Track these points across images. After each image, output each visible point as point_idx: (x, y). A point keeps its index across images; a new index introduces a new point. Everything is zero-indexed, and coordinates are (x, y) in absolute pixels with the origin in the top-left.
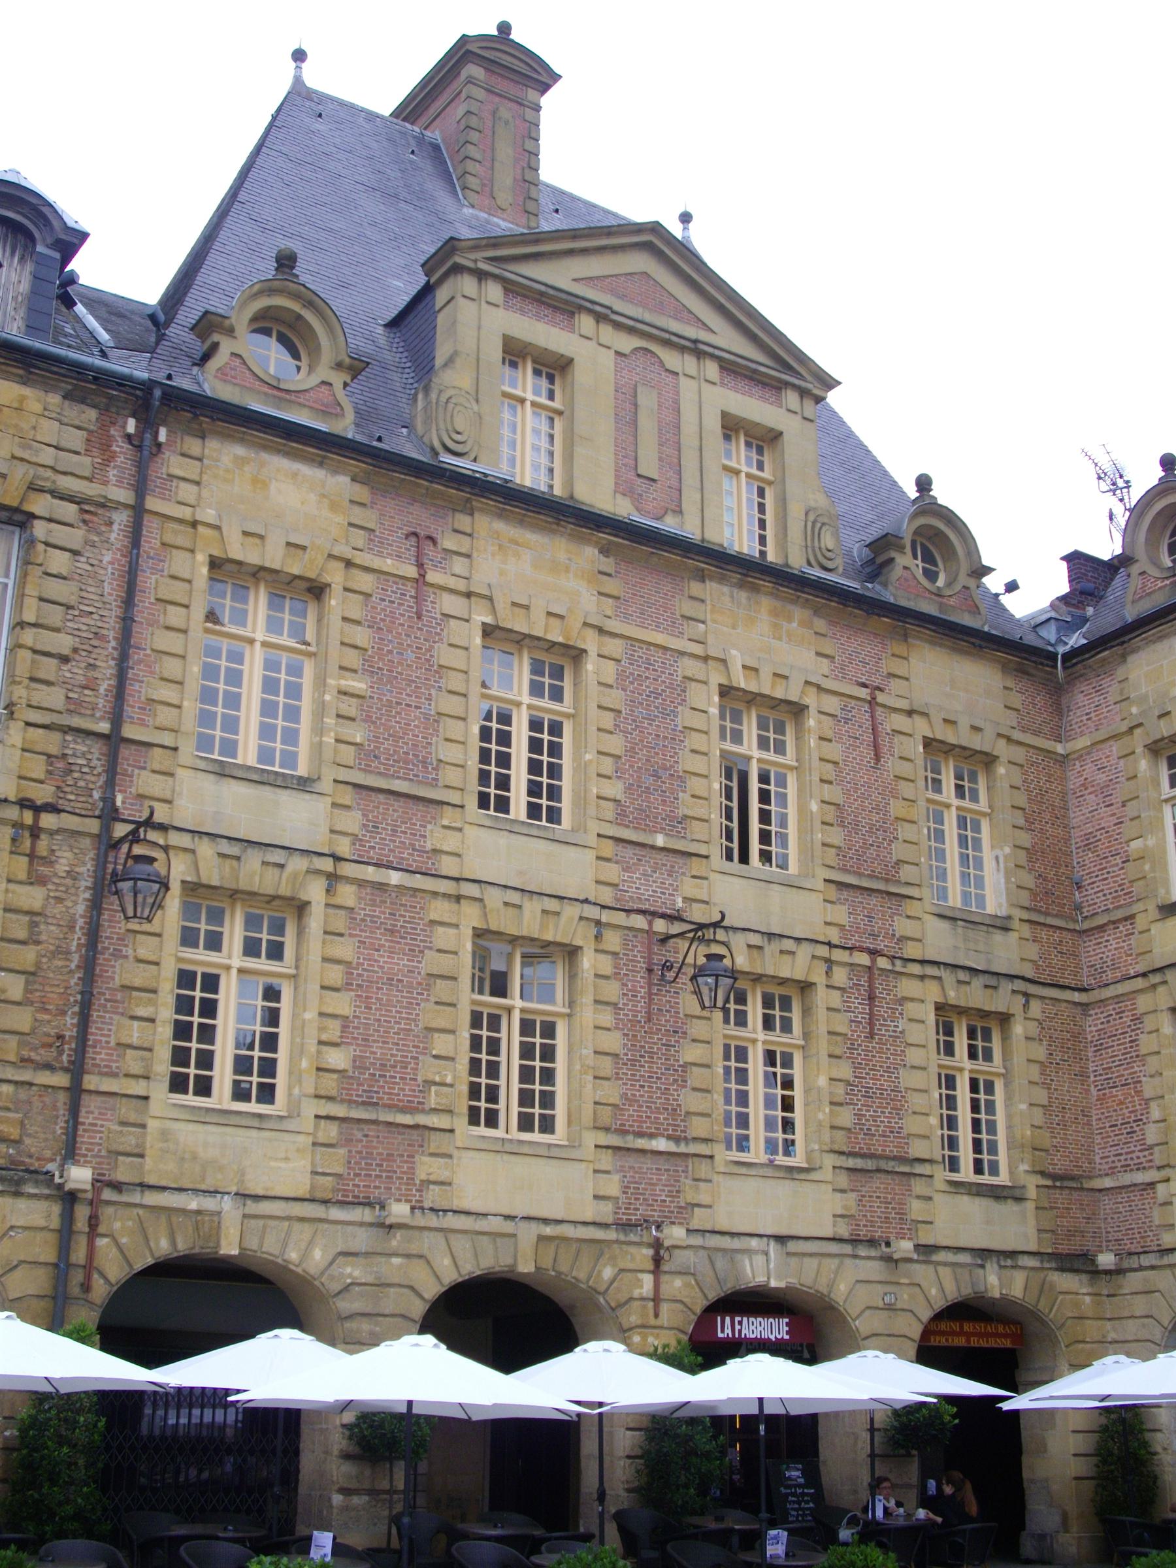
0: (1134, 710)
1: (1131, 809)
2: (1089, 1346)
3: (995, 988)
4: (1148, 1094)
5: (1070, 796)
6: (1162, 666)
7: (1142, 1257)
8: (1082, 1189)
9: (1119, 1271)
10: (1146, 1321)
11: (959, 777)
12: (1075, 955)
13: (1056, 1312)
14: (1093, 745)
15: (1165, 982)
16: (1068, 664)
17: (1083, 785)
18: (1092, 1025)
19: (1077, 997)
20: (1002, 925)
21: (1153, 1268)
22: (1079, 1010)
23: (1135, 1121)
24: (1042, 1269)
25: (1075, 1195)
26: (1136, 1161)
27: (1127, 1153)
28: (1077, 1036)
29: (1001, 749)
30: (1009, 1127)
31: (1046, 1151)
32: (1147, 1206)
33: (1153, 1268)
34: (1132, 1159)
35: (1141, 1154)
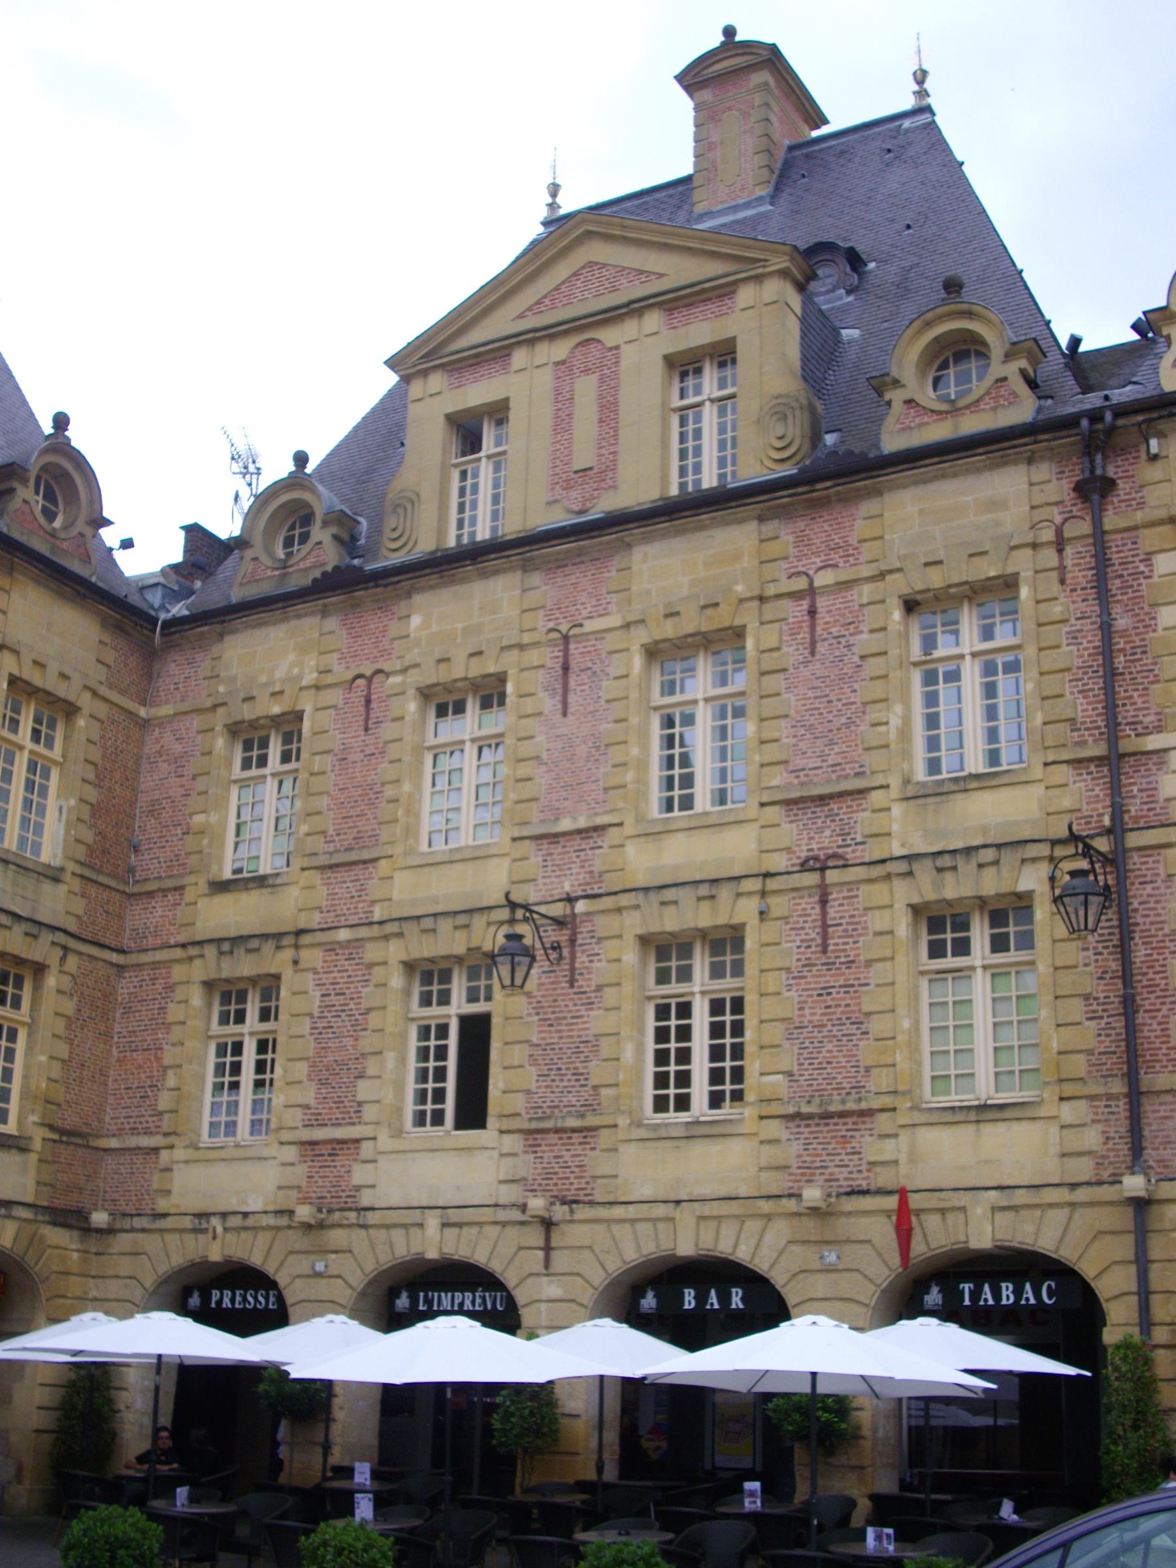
0: (221, 689)
2: (69, 1302)
3: (35, 937)
4: (167, 1060)
5: (144, 761)
6: (255, 652)
7: (135, 1219)
8: (87, 1147)
9: (110, 1231)
10: (129, 1281)
11: (38, 720)
12: (120, 917)
14: (176, 714)
15: (202, 956)
16: (167, 632)
17: (159, 752)
18: (125, 987)
19: (115, 957)
20: (54, 876)
21: (144, 1230)
22: (113, 971)
23: (150, 1086)
24: (35, 1221)
25: (80, 1152)
26: (145, 1125)
27: (137, 1117)
28: (108, 996)
29: (85, 701)
30: (26, 1077)
31: (59, 1105)
32: (147, 1171)
33: (144, 1230)
34: (141, 1123)
35: (150, 1119)
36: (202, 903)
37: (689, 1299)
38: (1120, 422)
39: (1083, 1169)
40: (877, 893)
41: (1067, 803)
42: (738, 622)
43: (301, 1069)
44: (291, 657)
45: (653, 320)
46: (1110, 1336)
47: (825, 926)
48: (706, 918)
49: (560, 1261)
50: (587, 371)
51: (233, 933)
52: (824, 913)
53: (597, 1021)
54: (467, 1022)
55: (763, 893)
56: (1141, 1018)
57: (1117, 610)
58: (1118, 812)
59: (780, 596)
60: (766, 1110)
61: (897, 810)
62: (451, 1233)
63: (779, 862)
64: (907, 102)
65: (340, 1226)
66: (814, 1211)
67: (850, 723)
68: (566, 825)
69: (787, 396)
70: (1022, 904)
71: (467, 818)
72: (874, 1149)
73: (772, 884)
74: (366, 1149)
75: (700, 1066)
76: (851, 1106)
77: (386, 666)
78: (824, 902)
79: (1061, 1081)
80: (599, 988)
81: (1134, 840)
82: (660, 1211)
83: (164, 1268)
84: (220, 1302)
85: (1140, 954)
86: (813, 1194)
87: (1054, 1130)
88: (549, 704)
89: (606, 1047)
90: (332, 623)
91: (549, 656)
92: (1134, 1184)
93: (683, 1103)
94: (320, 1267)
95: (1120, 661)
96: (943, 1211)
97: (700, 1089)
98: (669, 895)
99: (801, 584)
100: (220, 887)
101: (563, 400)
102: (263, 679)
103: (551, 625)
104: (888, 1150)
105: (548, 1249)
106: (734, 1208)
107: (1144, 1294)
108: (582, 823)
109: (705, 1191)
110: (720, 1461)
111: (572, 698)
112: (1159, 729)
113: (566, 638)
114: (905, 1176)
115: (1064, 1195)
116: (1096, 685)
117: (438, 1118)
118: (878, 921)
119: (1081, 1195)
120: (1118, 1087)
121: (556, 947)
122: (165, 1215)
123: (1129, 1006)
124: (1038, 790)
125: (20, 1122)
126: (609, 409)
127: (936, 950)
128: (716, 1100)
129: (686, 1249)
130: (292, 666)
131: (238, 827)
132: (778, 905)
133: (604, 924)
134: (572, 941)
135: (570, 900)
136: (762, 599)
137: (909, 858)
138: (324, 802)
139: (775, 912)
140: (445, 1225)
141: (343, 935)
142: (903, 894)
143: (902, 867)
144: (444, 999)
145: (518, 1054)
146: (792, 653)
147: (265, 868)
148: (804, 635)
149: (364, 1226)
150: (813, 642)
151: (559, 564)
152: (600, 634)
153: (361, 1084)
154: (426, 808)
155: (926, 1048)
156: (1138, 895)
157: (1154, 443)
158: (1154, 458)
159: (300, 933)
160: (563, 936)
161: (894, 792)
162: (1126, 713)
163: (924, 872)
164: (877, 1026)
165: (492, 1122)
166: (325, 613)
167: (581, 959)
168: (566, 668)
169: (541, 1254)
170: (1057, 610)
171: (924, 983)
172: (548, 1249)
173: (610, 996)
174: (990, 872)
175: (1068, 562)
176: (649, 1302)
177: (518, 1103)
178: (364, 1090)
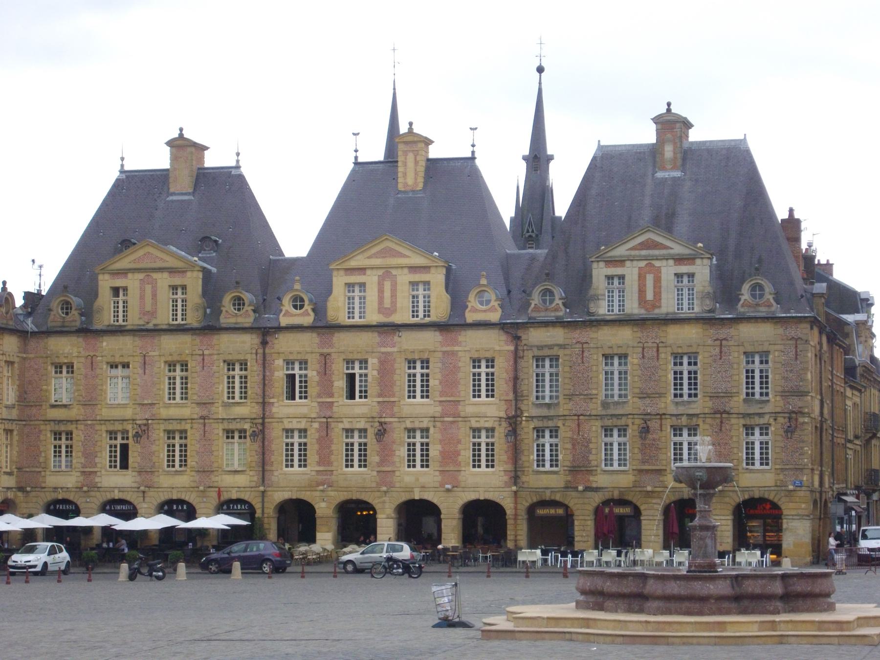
0: (49, 352)
1: (44, 378)
4: (41, 450)
9: (30, 492)
13: (17, 501)
19: (24, 423)
20: (13, 406)
21: (39, 491)
36: (48, 410)
37: (175, 507)
38: (270, 330)
39: (254, 484)
40: (216, 425)
41: (254, 411)
42: (186, 359)
43: (80, 454)
44: (69, 347)
45: (166, 275)
46: (257, 515)
47: (205, 432)
48: (179, 427)
49: (147, 499)
50: (148, 284)
51: (58, 419)
52: (205, 429)
53: (154, 448)
54: (122, 445)
55: (192, 423)
56: (266, 456)
57: (267, 371)
58: (264, 414)
59: (196, 355)
60: (192, 469)
61: (220, 408)
62: (121, 493)
63: (195, 416)
64: (234, 164)
65: (93, 491)
66: (202, 491)
67: (211, 387)
68: (146, 402)
69: (199, 304)
70: (245, 431)
71: (120, 395)
72: (214, 479)
73: (193, 421)
74: (98, 474)
75: (177, 458)
76: (209, 470)
77: (97, 354)
78: (204, 426)
79: (250, 467)
80: (154, 441)
81: (266, 420)
82: (169, 490)
83: (45, 500)
84: (59, 507)
85: (266, 443)
86: (201, 488)
87: (248, 476)
88: (141, 371)
89: (156, 454)
90: (81, 340)
91: (140, 359)
92: (262, 488)
93: (173, 466)
94: (88, 500)
95: (267, 382)
96: (227, 491)
97: (177, 463)
98: (171, 421)
99: (201, 352)
100: (53, 406)
101: (142, 290)
102: (61, 352)
103: (141, 352)
104: (217, 479)
105: (144, 497)
106: (185, 489)
107: (263, 508)
108: (150, 402)
109: (179, 486)
110: (177, 539)
111: (147, 371)
112: (273, 398)
113: (145, 356)
114: (220, 484)
115: (249, 489)
116: (261, 386)
117: (115, 467)
118: (216, 431)
119: (253, 489)
120: (261, 469)
121: (144, 431)
122: (45, 488)
123: (264, 454)
124: (249, 408)
125: (10, 468)
126: (154, 295)
127: (228, 437)
128: (181, 466)
129: (175, 497)
130: (69, 350)
131: (55, 389)
132: (195, 426)
133: (155, 426)
134: (148, 429)
135: (147, 420)
136: (192, 355)
137: (223, 419)
138: (81, 388)
139: (194, 427)
140: (119, 491)
141: (89, 422)
142: (221, 427)
143: (221, 421)
144: (116, 439)
145: (136, 454)
146: (198, 368)
147: (64, 402)
148: (201, 365)
149: (99, 491)
150: (203, 367)
151: (143, 336)
152: (153, 356)
153: (96, 459)
154: (109, 391)
155: (225, 458)
156: (267, 431)
157: (276, 336)
158: (276, 338)
159: (77, 421)
160: (145, 428)
161: (220, 404)
162: (267, 393)
163: (225, 422)
164: (215, 453)
165: (130, 469)
166: (78, 337)
167: (150, 434)
168: (145, 363)
169: (142, 498)
170: (255, 369)
171: (225, 444)
172: (144, 497)
173: (157, 443)
174: (238, 424)
175: (258, 358)
176: (166, 508)
177: (136, 465)
178: (97, 460)
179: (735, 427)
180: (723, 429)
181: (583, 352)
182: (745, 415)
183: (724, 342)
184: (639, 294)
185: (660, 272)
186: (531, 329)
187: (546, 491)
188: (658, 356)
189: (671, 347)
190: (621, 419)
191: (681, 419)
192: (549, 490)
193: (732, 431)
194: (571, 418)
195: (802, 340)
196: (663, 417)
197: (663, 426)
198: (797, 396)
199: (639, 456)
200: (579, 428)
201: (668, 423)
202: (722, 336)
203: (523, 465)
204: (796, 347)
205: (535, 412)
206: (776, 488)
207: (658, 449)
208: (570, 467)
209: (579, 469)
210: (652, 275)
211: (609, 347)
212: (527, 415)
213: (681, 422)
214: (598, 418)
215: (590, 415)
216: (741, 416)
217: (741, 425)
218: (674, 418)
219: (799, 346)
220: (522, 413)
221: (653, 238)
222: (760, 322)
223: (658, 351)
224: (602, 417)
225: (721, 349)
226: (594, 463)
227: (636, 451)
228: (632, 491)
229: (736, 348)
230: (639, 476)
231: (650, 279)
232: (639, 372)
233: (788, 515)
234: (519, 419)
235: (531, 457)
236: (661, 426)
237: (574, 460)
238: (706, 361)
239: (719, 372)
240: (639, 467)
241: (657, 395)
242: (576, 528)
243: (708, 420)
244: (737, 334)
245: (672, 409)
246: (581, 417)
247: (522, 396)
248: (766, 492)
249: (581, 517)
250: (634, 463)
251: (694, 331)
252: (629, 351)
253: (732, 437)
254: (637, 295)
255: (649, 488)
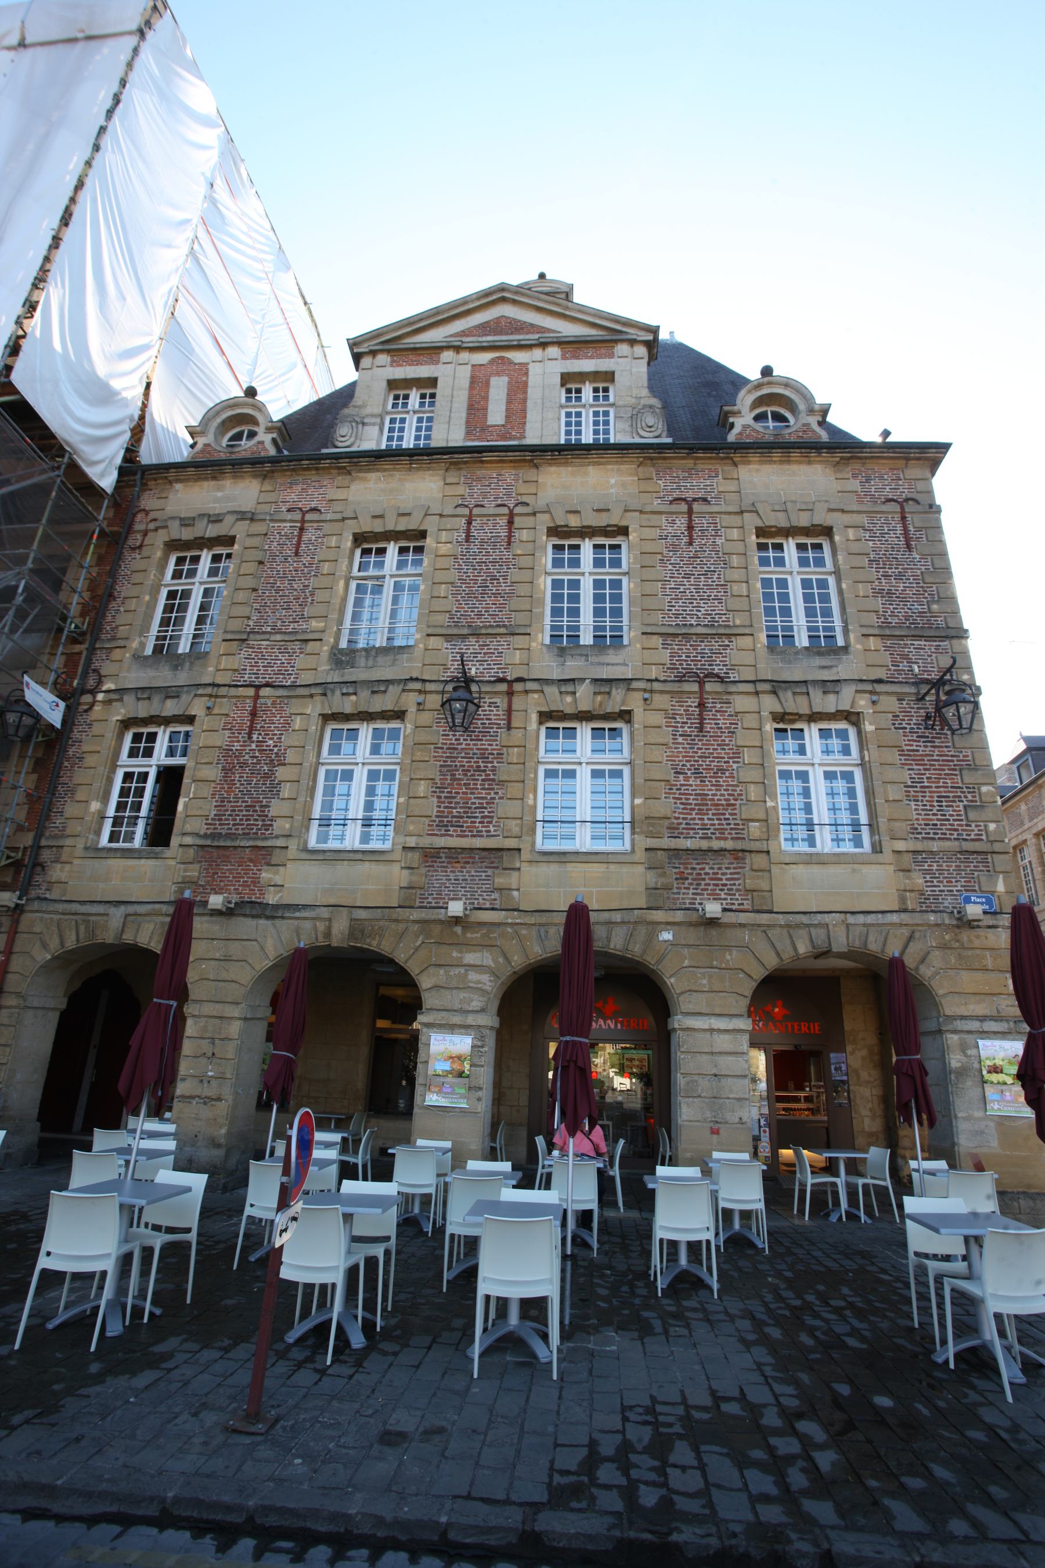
179: (750, 721)
180: (708, 727)
181: (302, 529)
182: (777, 687)
183: (696, 507)
184: (469, 414)
185: (526, 374)
186: (178, 486)
187: (112, 910)
188: (510, 537)
189: (549, 512)
190: (385, 692)
191: (574, 693)
192: (122, 909)
193: (740, 732)
194: (233, 692)
195: (918, 503)
196: (518, 687)
197: (514, 714)
198: (928, 638)
199: (432, 807)
200: (252, 722)
201: (530, 705)
202: (689, 495)
203: (64, 828)
204: (903, 518)
205: (135, 677)
206: (905, 917)
207: (493, 782)
208: (205, 836)
209: (229, 843)
210: (506, 379)
211: (375, 517)
212: (112, 686)
213: (575, 701)
214: (313, 691)
215: (294, 686)
216: (767, 687)
217: (765, 714)
218: (552, 691)
219: (909, 517)
220: (100, 682)
221: (511, 315)
222: (800, 463)
223: (511, 523)
224: (324, 688)
225: (690, 520)
226: (282, 826)
227: (422, 788)
228: (397, 921)
229: (736, 520)
230: (423, 870)
231: (498, 389)
232: (453, 575)
233: (963, 1018)
234: (87, 698)
235: (95, 806)
236: (509, 711)
237: (219, 817)
238: (649, 547)
239: (687, 576)
240: (426, 842)
241: (503, 630)
242: (187, 1047)
243: (661, 701)
244: (733, 489)
245: (547, 666)
246: (265, 692)
247: (114, 639)
248: (872, 929)
249: (208, 1009)
250: (411, 828)
251: (613, 481)
252: (430, 525)
253: (737, 755)
254: (464, 415)
255: (456, 908)
